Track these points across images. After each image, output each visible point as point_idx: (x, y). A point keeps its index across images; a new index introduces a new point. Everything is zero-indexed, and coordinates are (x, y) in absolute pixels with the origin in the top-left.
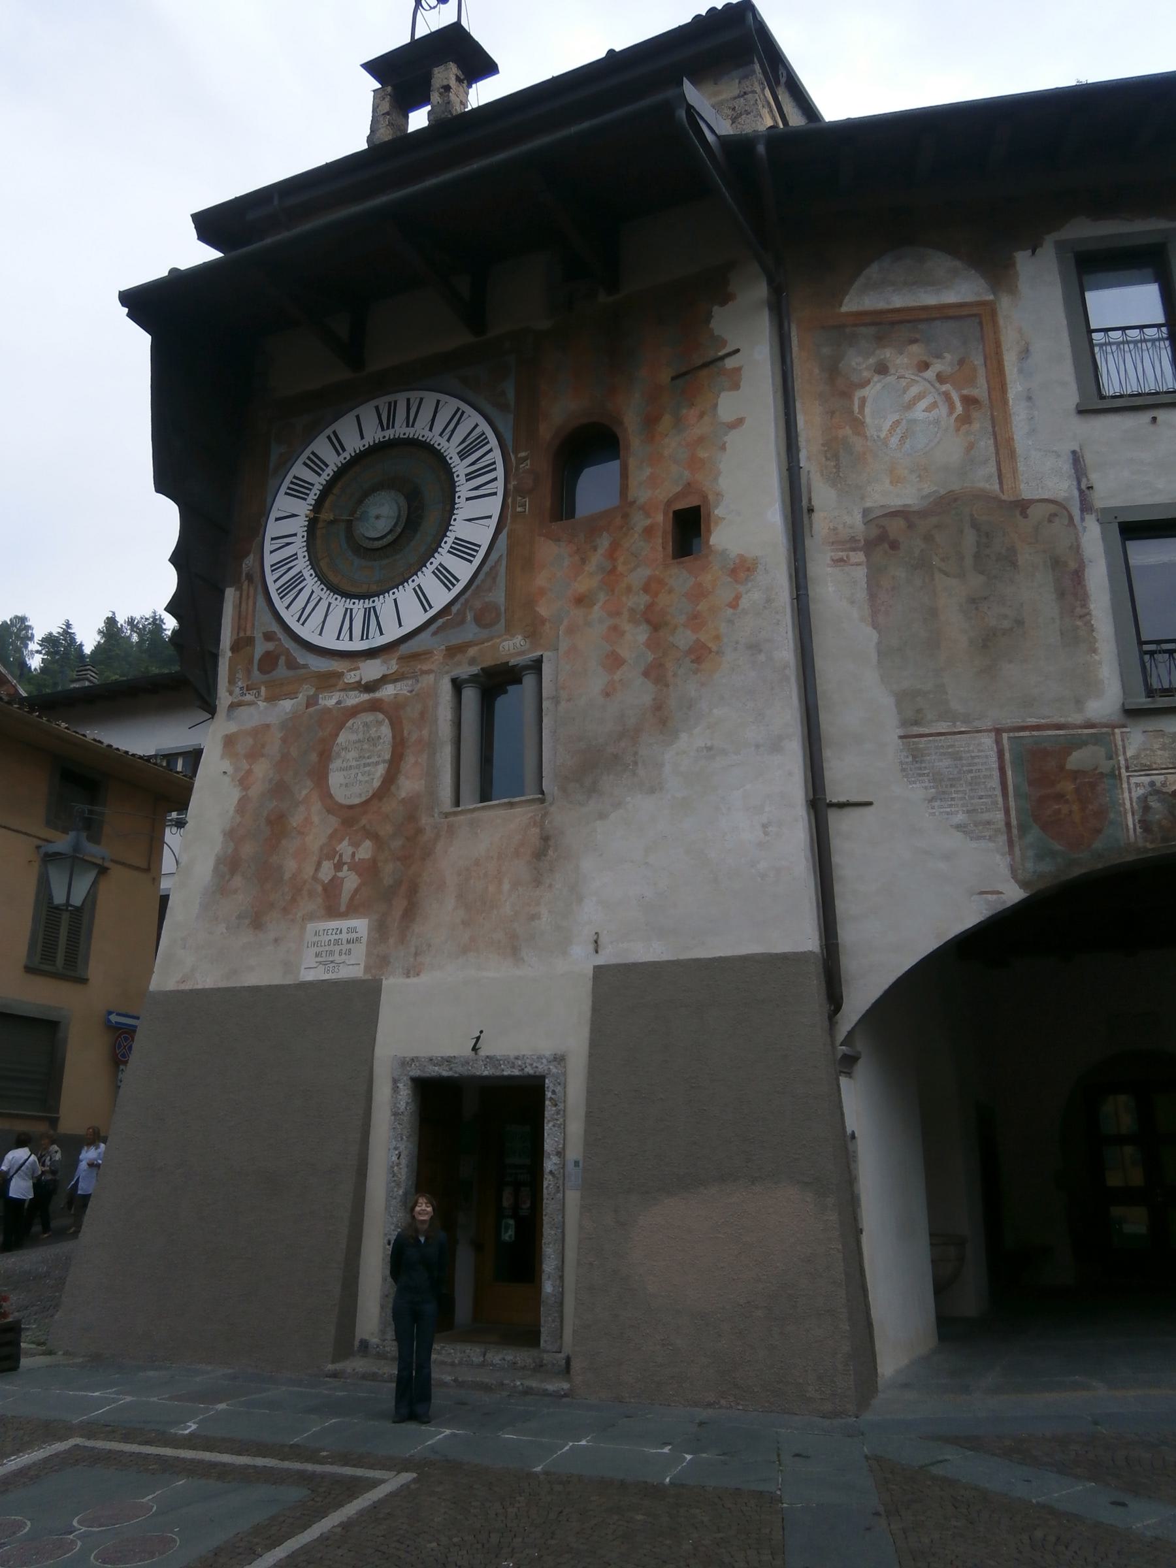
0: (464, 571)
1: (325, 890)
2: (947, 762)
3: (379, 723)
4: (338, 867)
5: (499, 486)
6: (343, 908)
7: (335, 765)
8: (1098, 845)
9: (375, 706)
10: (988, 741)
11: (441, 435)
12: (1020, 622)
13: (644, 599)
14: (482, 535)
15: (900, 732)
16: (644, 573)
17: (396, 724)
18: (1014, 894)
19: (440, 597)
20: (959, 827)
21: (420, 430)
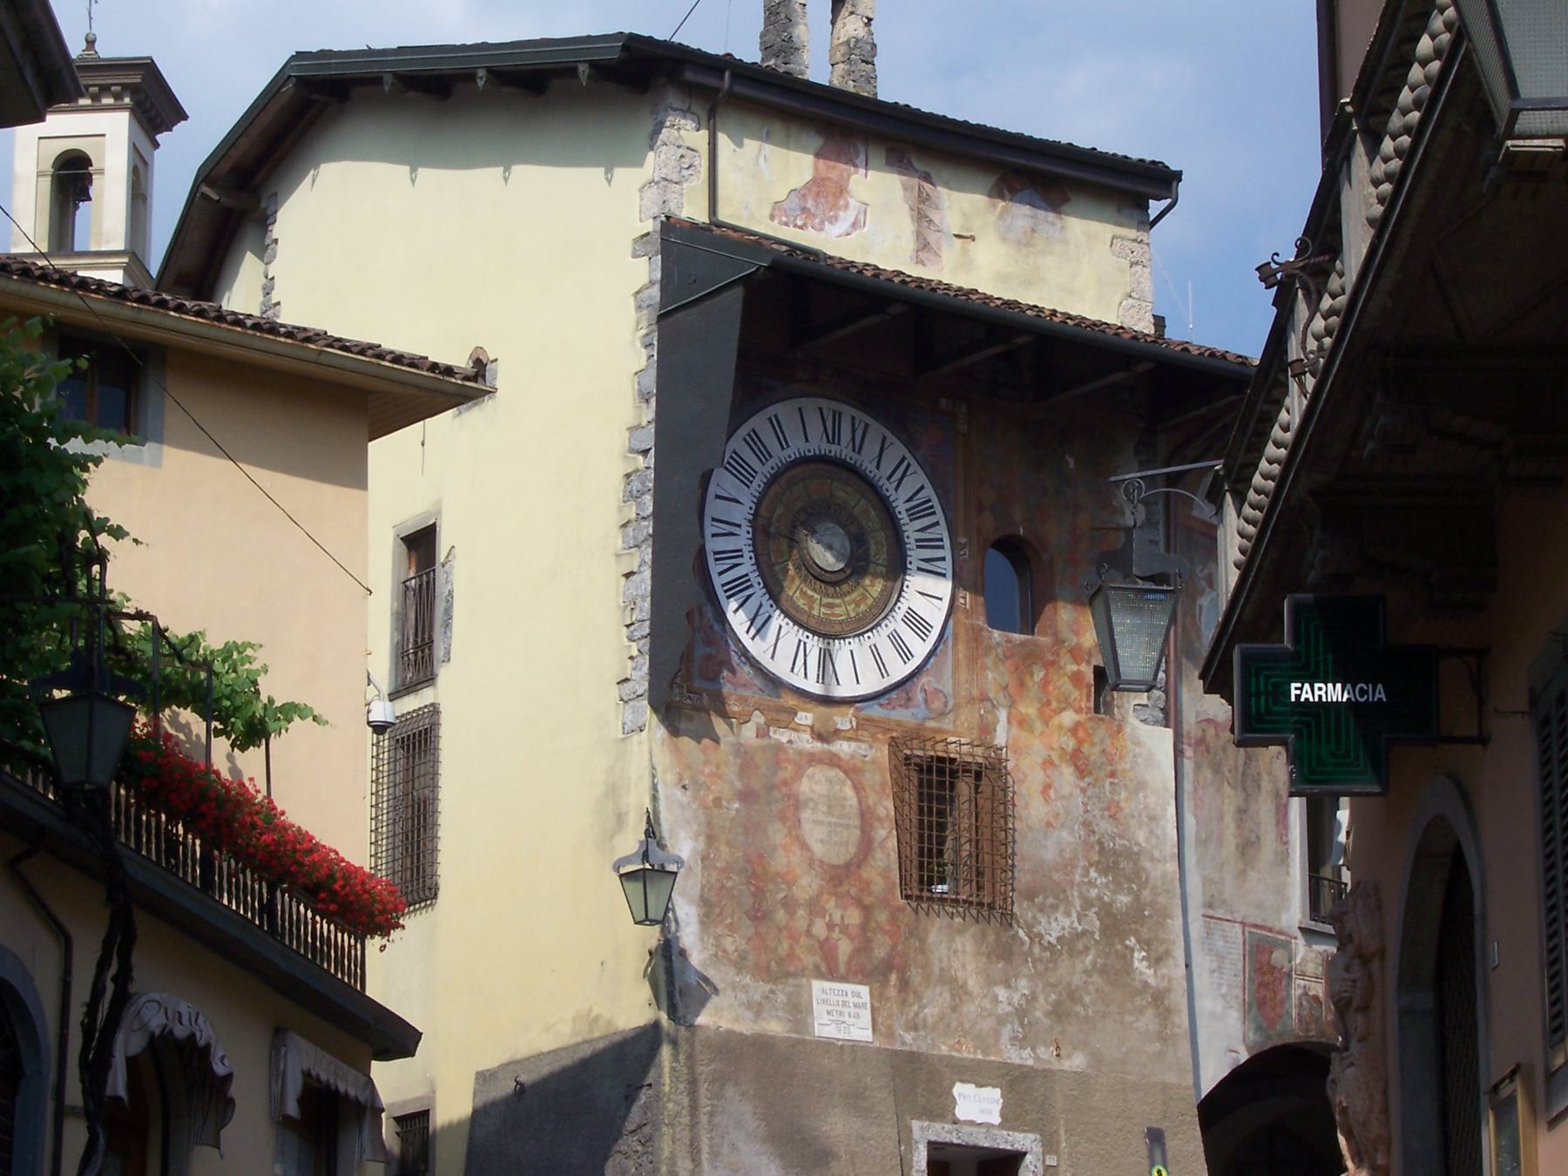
0: (920, 649)
1: (822, 947)
2: (1221, 943)
3: (843, 784)
4: (831, 926)
5: (947, 566)
6: (842, 969)
7: (806, 815)
8: (1279, 1027)
9: (833, 761)
10: (1238, 928)
11: (889, 478)
12: (1258, 838)
13: (1070, 743)
14: (935, 615)
15: (1202, 911)
16: (1068, 718)
17: (858, 788)
18: (1244, 1056)
19: (899, 671)
20: (1223, 996)
21: (866, 462)
